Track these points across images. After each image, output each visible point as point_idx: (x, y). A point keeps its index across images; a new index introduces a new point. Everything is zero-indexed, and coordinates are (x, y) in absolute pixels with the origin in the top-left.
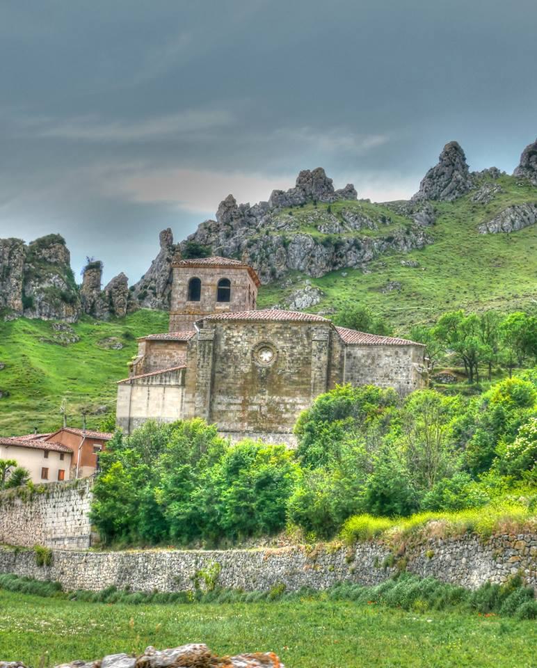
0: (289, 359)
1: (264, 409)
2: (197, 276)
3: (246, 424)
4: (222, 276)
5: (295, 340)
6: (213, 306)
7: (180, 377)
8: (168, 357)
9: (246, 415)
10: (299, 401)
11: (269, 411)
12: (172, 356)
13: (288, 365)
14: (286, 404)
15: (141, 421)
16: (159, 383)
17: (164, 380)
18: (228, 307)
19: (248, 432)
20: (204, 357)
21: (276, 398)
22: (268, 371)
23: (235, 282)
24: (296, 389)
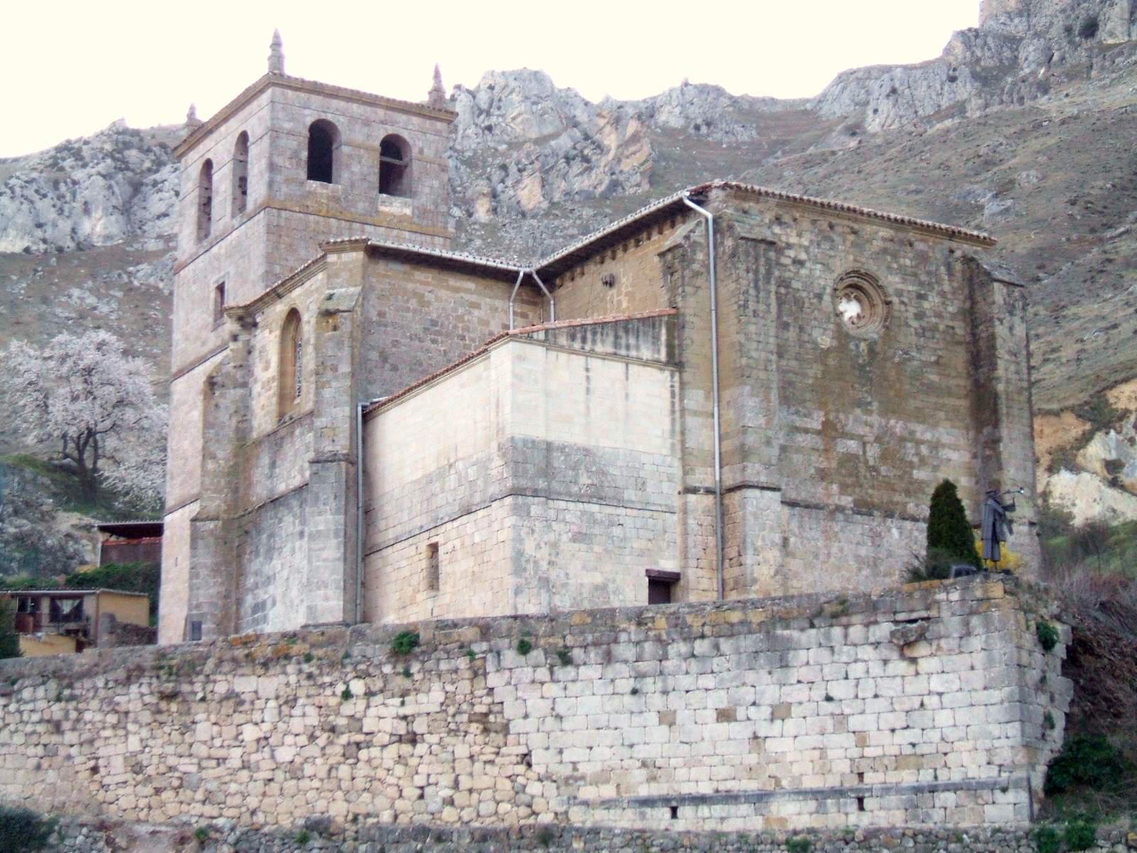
0: (915, 324)
1: (873, 452)
2: (329, 117)
3: (835, 487)
4: (391, 130)
5: (923, 278)
6: (373, 202)
7: (664, 337)
8: (413, 304)
9: (834, 464)
10: (945, 439)
11: (884, 457)
12: (423, 303)
13: (914, 339)
14: (919, 443)
15: (574, 458)
16: (610, 349)
17: (623, 342)
18: (408, 211)
19: (839, 509)
20: (756, 287)
21: (898, 426)
22: (872, 351)
23: (421, 151)
24: (938, 408)
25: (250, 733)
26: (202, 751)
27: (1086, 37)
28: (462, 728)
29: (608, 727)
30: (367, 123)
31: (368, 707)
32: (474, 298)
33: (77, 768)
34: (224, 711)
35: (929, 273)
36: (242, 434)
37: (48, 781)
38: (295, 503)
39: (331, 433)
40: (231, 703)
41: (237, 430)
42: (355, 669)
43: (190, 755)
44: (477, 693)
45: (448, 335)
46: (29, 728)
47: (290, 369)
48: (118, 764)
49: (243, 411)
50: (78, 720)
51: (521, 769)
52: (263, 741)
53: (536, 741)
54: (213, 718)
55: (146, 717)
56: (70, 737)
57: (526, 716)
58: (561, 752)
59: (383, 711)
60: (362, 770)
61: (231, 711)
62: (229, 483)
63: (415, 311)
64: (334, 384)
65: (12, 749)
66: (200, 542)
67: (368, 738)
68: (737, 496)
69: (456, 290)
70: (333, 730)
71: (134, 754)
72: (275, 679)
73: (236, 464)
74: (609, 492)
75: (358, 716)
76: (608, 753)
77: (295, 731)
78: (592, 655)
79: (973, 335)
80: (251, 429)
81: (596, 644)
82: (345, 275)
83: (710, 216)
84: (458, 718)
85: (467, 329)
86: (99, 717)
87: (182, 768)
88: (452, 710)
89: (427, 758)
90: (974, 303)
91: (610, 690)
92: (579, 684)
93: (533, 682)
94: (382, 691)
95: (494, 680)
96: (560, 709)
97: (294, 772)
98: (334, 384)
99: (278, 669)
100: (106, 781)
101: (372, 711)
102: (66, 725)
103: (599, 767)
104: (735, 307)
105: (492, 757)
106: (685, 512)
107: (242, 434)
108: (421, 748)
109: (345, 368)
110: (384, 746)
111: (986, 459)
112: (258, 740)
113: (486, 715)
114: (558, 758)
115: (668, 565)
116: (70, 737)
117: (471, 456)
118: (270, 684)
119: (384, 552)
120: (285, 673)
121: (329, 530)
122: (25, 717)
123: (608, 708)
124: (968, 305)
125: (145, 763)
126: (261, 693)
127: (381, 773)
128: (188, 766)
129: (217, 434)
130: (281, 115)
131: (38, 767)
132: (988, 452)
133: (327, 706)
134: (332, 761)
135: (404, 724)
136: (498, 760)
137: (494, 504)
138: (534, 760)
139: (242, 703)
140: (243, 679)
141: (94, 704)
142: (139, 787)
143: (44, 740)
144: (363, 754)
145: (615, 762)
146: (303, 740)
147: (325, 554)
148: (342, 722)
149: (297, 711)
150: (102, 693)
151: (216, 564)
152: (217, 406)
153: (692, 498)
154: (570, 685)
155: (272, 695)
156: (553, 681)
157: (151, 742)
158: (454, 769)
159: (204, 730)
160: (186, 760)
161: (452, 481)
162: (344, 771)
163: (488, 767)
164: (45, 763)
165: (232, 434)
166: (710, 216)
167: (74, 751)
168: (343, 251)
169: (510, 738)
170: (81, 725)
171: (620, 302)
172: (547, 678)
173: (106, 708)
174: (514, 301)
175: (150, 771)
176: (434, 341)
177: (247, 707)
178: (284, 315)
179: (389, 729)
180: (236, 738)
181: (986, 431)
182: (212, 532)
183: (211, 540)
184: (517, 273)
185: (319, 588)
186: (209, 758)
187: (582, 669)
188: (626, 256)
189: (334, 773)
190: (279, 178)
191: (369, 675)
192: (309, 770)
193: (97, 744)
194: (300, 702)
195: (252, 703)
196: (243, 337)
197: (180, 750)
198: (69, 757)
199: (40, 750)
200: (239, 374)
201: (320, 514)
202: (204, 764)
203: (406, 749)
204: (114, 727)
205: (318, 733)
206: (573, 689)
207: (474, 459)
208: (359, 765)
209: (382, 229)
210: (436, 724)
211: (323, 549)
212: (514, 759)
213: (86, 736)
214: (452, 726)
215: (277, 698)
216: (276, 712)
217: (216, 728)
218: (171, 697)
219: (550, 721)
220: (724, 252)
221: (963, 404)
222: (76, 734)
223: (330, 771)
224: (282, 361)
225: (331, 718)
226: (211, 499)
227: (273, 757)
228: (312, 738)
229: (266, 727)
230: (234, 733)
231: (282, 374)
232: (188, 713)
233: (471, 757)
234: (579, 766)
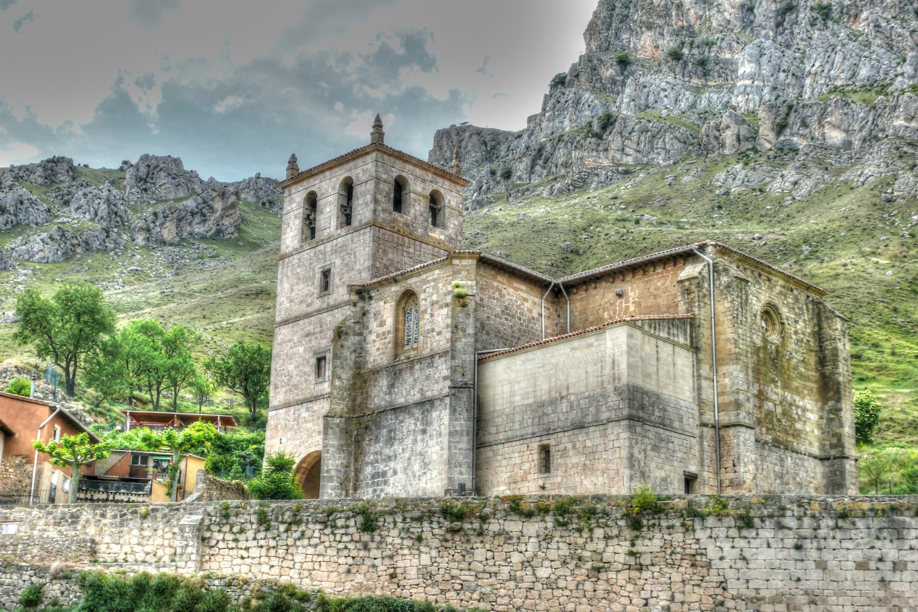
0: (794, 337)
1: (779, 410)
2: (405, 174)
3: (764, 430)
4: (435, 187)
5: (797, 311)
6: (426, 229)
7: (688, 331)
8: (497, 295)
9: (763, 416)
10: (809, 407)
11: (784, 413)
12: (502, 296)
13: (793, 346)
14: (798, 407)
15: (653, 399)
16: (666, 336)
17: (671, 331)
18: (442, 237)
19: (766, 443)
20: (742, 307)
21: (789, 396)
22: (777, 352)
23: (449, 201)
24: (805, 387)
25: (516, 558)
26: (480, 567)
28: (677, 563)
29: (779, 568)
30: (424, 181)
31: (607, 545)
32: (525, 295)
33: (380, 573)
34: (496, 542)
35: (799, 308)
36: (359, 366)
37: (356, 580)
38: (417, 413)
39: (461, 370)
40: (502, 538)
41: (356, 362)
42: (597, 522)
43: (469, 570)
44: (688, 542)
45: (513, 316)
46: (341, 546)
47: (401, 327)
48: (413, 573)
49: (360, 351)
50: (381, 542)
51: (720, 591)
52: (527, 564)
53: (730, 574)
54: (488, 546)
55: (435, 543)
56: (375, 553)
57: (722, 558)
58: (748, 581)
59: (618, 549)
60: (602, 586)
61: (502, 543)
62: (350, 395)
63: (497, 299)
64: (463, 340)
65: (327, 558)
66: (330, 431)
67: (606, 565)
68: (732, 431)
69: (517, 289)
70: (580, 559)
71: (426, 567)
72: (537, 525)
73: (355, 384)
74: (667, 422)
75: (599, 551)
76: (780, 584)
77: (551, 558)
78: (767, 523)
79: (821, 347)
80: (366, 362)
81: (771, 516)
82: (464, 273)
83: (711, 262)
84: (674, 557)
85: (522, 313)
86: (398, 541)
87: (463, 578)
88: (669, 551)
89: (650, 581)
90: (821, 328)
91: (781, 546)
92: (758, 540)
93: (727, 537)
94: (617, 537)
95: (699, 534)
96: (747, 554)
97: (550, 584)
98: (463, 340)
99: (539, 518)
100: (402, 583)
101: (610, 549)
102: (372, 545)
103: (774, 592)
104: (730, 317)
105: (699, 582)
106: (701, 437)
107: (359, 366)
108: (646, 574)
109: (471, 331)
110: (619, 571)
111: (830, 420)
112: (523, 563)
113: (694, 555)
114: (745, 586)
115: (693, 468)
116: (375, 553)
117: (584, 393)
118: (533, 527)
119: (495, 447)
120: (543, 521)
121: (462, 431)
122: (338, 538)
123: (780, 556)
124: (816, 329)
125: (433, 573)
126: (525, 532)
127: (616, 588)
128: (468, 577)
129: (342, 363)
130: (380, 169)
131: (349, 571)
132: (832, 416)
133: (576, 543)
134: (579, 579)
135: (633, 558)
136: (703, 584)
137: (610, 424)
138: (729, 586)
139: (511, 538)
140: (512, 523)
141: (394, 533)
142: (428, 589)
143: (354, 553)
144: (603, 576)
145: (786, 589)
146: (557, 564)
147: (460, 446)
148: (587, 554)
149: (553, 545)
150: (400, 525)
151: (341, 446)
152: (342, 346)
153: (705, 429)
154: (752, 540)
155: (534, 535)
156: (740, 537)
157: (438, 560)
158: (670, 588)
159: (480, 554)
160: (467, 573)
161: (564, 406)
162: (588, 586)
163: (696, 589)
164: (354, 570)
165: (352, 364)
166: (711, 262)
167: (377, 562)
168: (464, 258)
169: (713, 572)
170: (384, 545)
171: (627, 308)
172: (737, 536)
173: (403, 535)
174: (546, 300)
175: (439, 578)
176: (506, 319)
177: (515, 540)
178: (399, 294)
179: (622, 560)
180: (506, 560)
181: (830, 403)
182: (338, 425)
183: (337, 430)
184: (550, 283)
185: (456, 467)
186: (484, 572)
187: (760, 531)
188: (633, 280)
189: (580, 587)
190: (379, 208)
191: (608, 526)
192: (562, 583)
193: (395, 559)
194: (556, 539)
195: (519, 538)
196: (360, 304)
197: (461, 566)
198: (374, 566)
199: (350, 561)
200: (357, 327)
201: (456, 420)
202: (480, 575)
203: (634, 574)
204: (409, 548)
205: (568, 560)
206: (755, 543)
207: (586, 394)
208: (600, 582)
209: (430, 247)
210: (657, 559)
211: (459, 442)
212: (715, 585)
213: (388, 553)
214: (669, 561)
215: (538, 536)
216: (537, 545)
217: (490, 554)
218: (454, 531)
219: (740, 564)
220: (720, 284)
221: (814, 386)
222: (380, 551)
223: (577, 585)
224: (396, 322)
225: (579, 551)
226: (338, 404)
227: (534, 574)
228: (564, 563)
229: (529, 554)
230: (504, 557)
231: (396, 330)
232: (468, 541)
233: (683, 581)
234: (761, 591)
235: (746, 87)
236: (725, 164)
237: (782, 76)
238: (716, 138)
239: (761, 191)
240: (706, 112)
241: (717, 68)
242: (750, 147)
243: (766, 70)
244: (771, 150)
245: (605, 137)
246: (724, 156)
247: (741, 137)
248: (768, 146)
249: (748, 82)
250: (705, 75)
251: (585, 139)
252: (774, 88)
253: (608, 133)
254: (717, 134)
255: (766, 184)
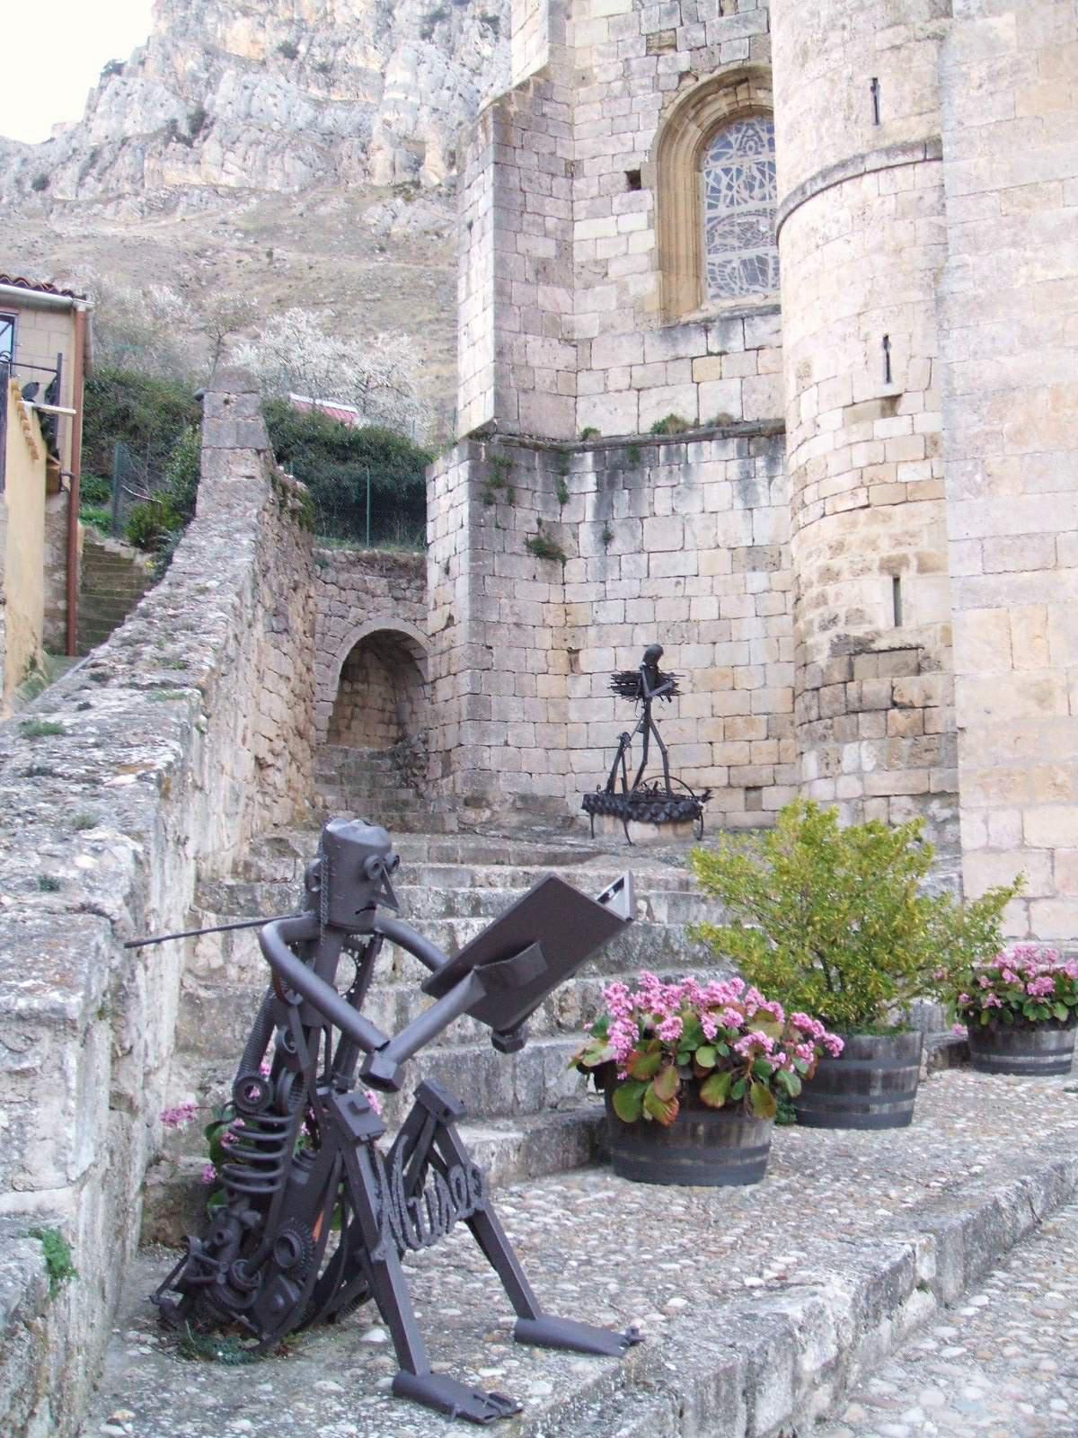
27: (37, 190)
235: (396, 101)
236: (376, 197)
237: (446, 93)
238: (360, 161)
239: (437, 234)
240: (332, 133)
241: (345, 77)
242: (408, 179)
243: (424, 82)
244: (440, 185)
245: (196, 144)
246: (374, 188)
247: (397, 165)
248: (436, 181)
249: (401, 96)
250: (330, 85)
251: (166, 145)
252: (435, 110)
253: (201, 138)
254: (363, 156)
255: (443, 228)
